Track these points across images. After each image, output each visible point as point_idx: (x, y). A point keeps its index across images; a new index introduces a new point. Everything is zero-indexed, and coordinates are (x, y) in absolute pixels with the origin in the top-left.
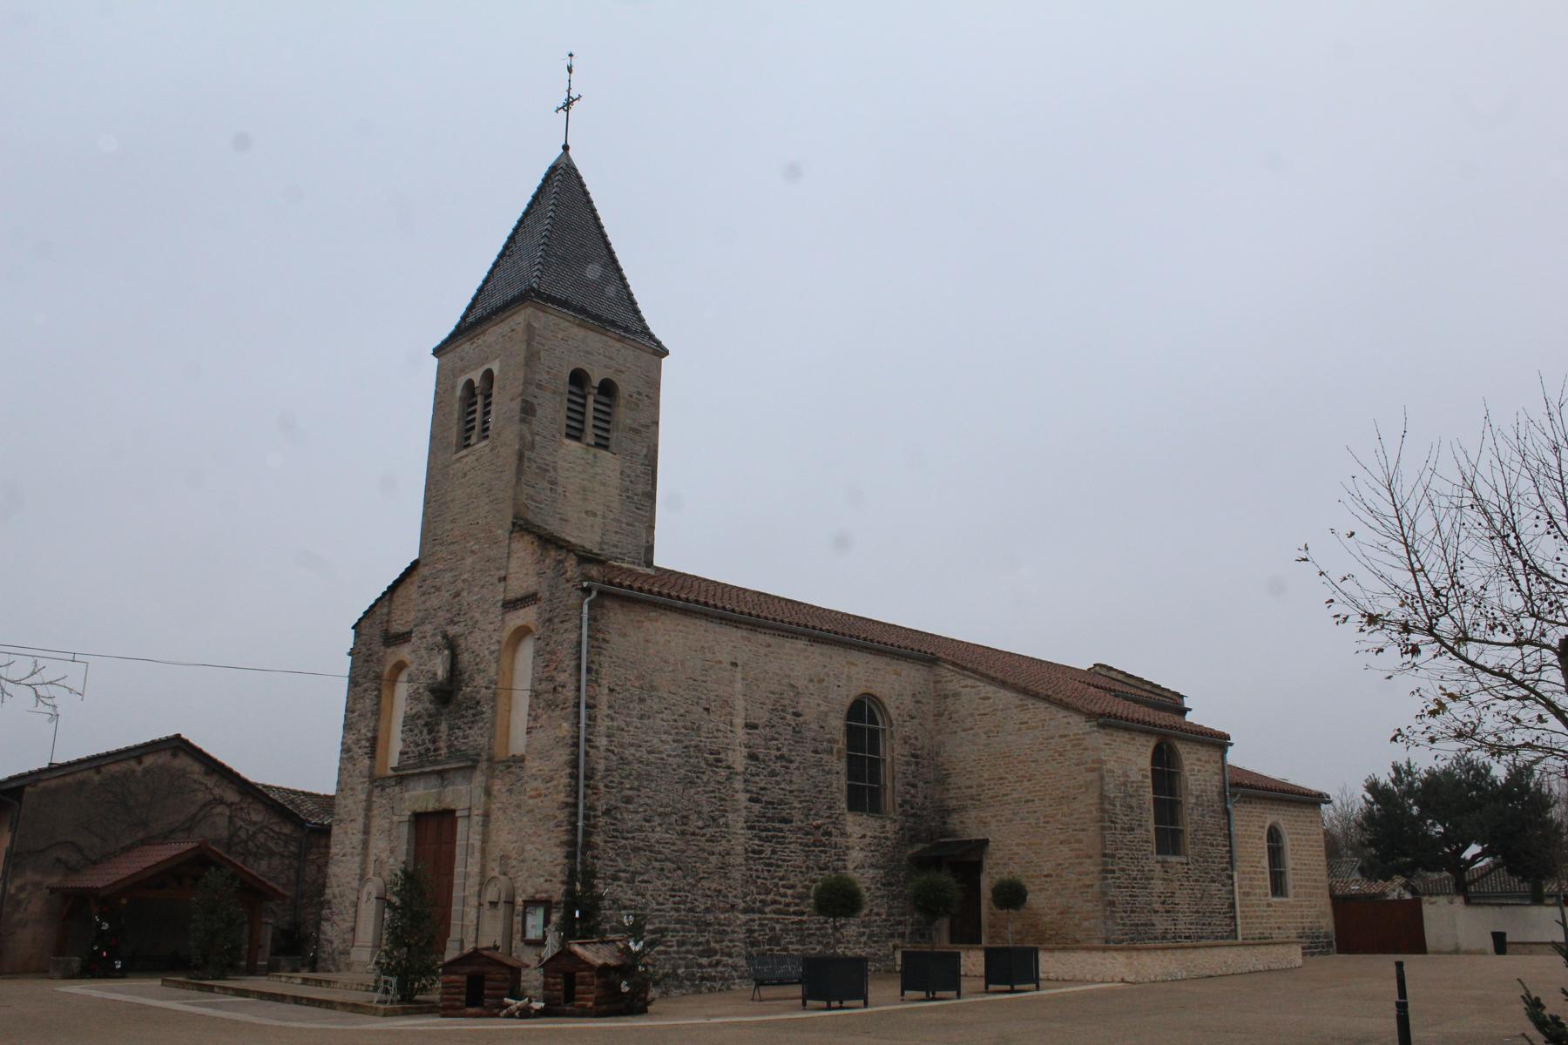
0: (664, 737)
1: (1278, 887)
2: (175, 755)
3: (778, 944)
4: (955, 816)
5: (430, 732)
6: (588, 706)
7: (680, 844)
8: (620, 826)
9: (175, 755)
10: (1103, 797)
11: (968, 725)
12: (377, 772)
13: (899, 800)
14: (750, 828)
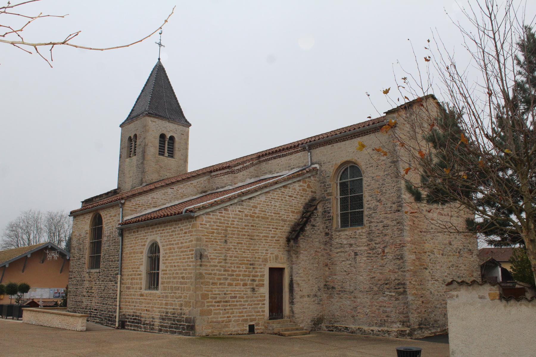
1: (153, 280)
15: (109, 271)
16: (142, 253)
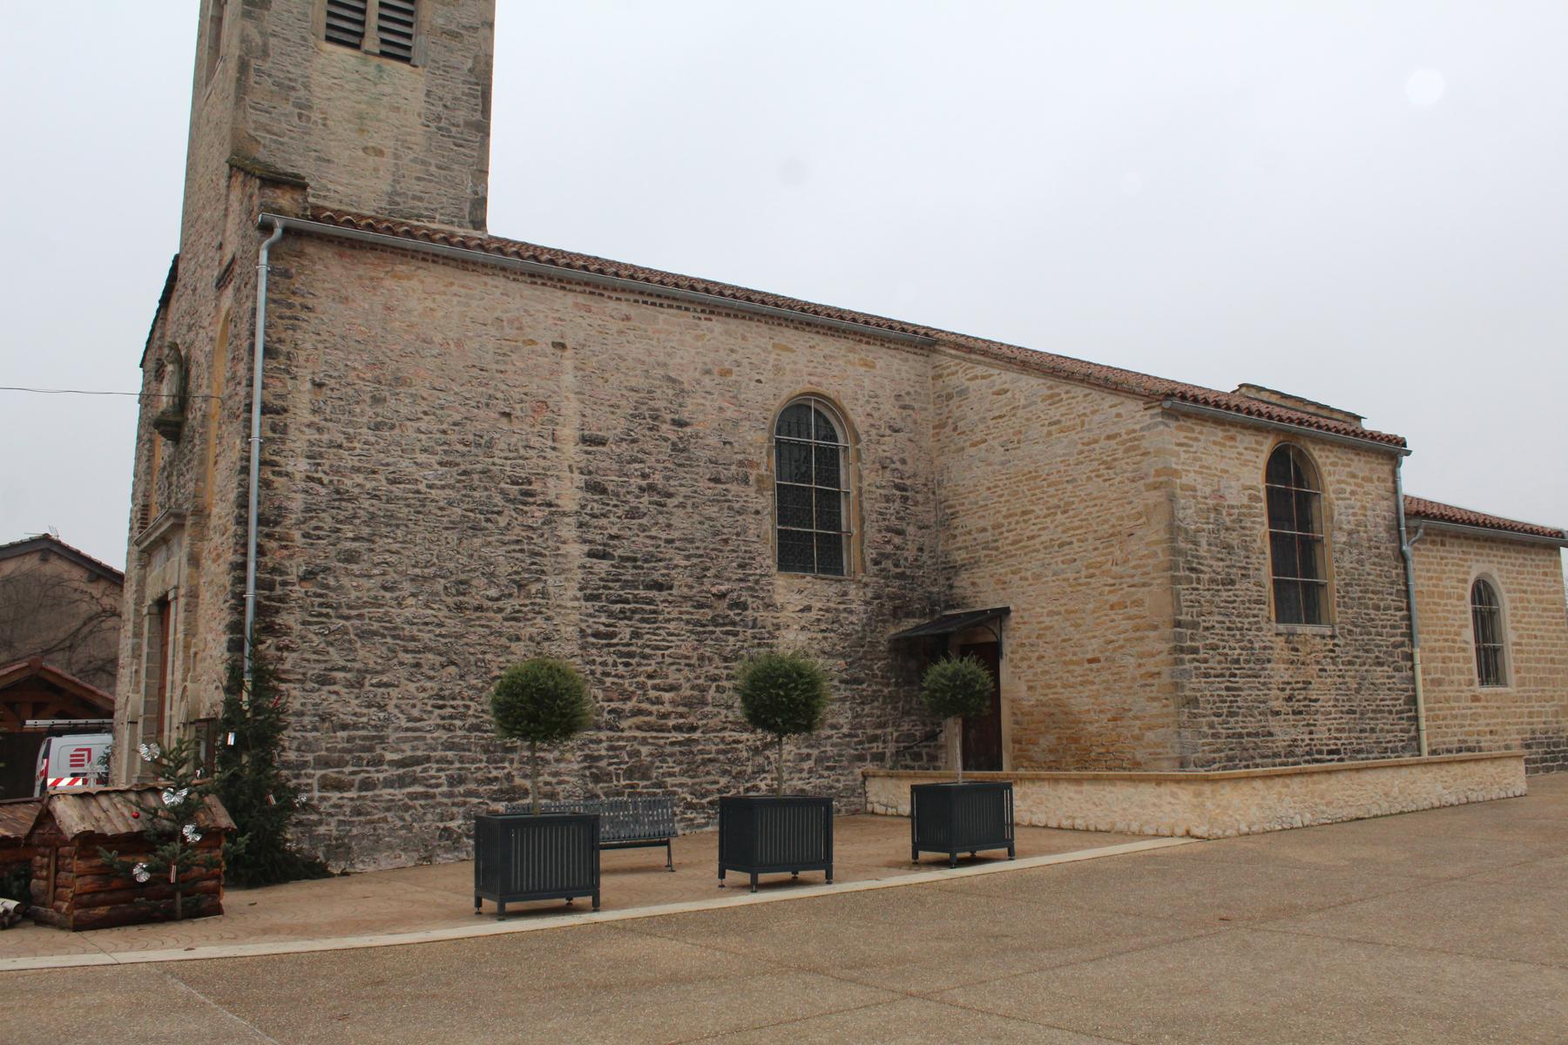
0: (421, 458)
1: (1490, 667)
2: (44, 560)
3: (645, 777)
4: (964, 575)
6: (265, 410)
7: (453, 625)
8: (333, 597)
9: (44, 560)
10: (1174, 529)
11: (978, 437)
13: (871, 554)
14: (588, 598)
15: (1369, 634)
16: (1461, 598)
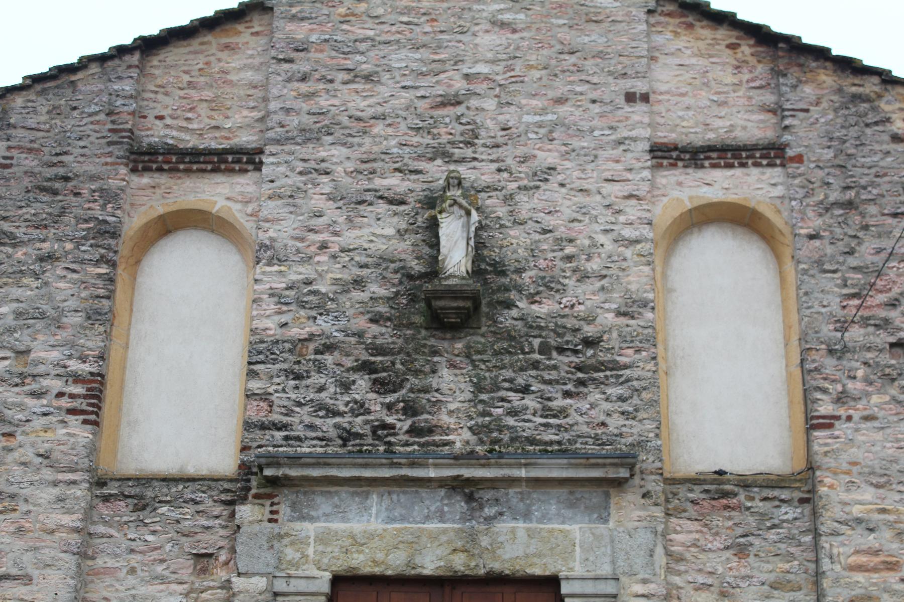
5: (381, 386)
12: (106, 466)
